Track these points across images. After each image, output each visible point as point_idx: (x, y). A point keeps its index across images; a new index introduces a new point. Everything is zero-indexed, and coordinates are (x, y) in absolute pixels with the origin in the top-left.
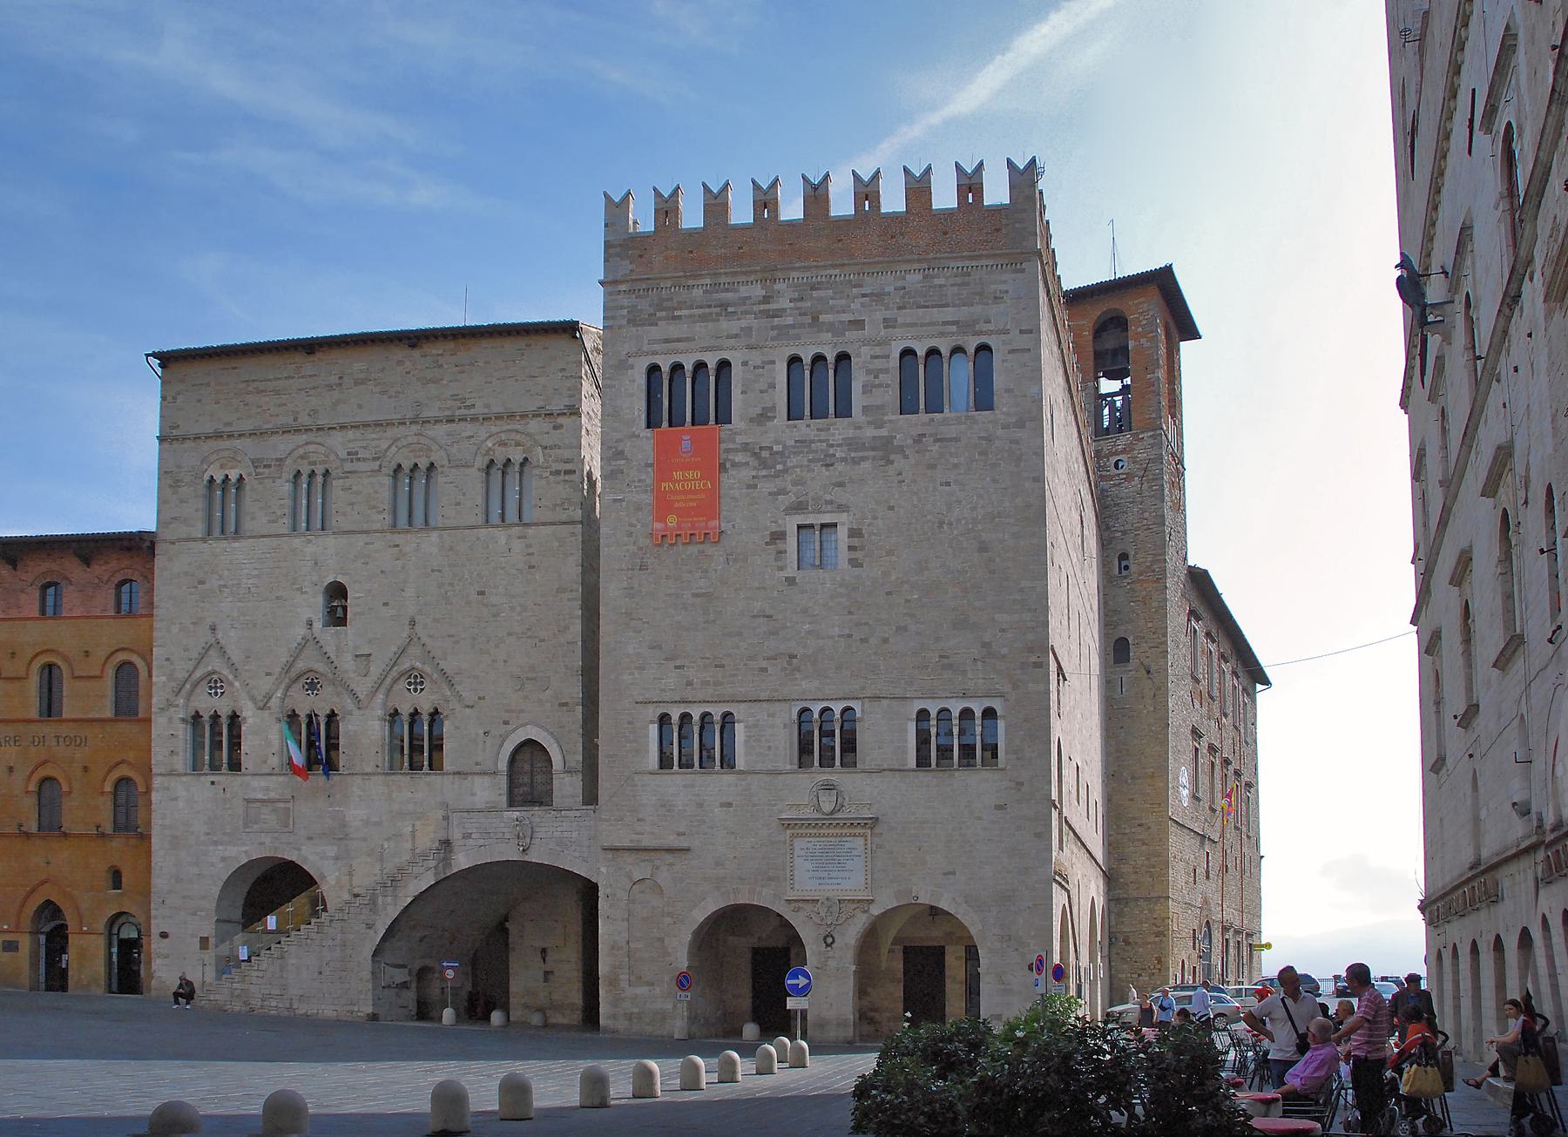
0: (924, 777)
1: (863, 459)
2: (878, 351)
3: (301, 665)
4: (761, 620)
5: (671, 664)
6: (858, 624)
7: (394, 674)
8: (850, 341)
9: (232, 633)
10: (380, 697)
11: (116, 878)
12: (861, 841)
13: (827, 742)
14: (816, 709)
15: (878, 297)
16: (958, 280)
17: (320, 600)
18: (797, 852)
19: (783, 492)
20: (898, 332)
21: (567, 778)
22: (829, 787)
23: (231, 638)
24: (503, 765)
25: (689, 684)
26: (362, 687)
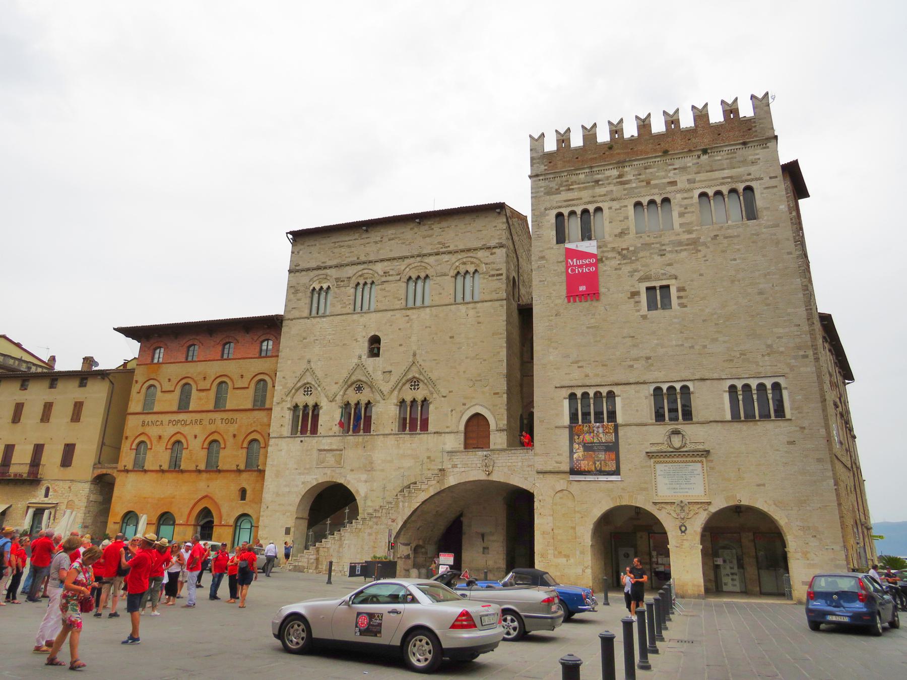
0: (736, 425)
1: (681, 250)
2: (685, 195)
3: (354, 378)
4: (627, 339)
5: (576, 365)
6: (686, 339)
7: (404, 381)
8: (669, 192)
9: (319, 363)
11: (243, 493)
12: (699, 465)
13: (673, 405)
14: (665, 387)
15: (684, 169)
16: (730, 156)
17: (366, 344)
18: (658, 472)
19: (636, 271)
20: (697, 185)
21: (498, 434)
22: (676, 432)
23: (319, 367)
24: (462, 427)
25: (587, 376)
26: (386, 388)
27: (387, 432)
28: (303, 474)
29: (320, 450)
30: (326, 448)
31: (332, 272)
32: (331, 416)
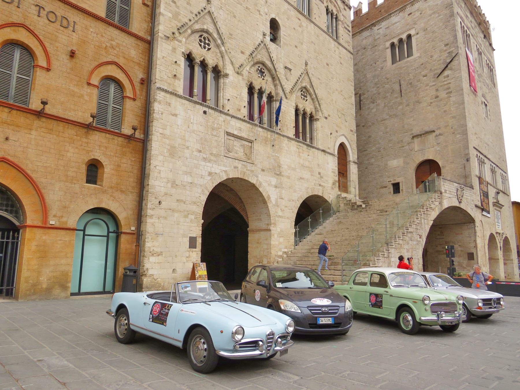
24: (336, 153)
28: (210, 161)
29: (228, 134)
30: (236, 133)
32: (234, 92)
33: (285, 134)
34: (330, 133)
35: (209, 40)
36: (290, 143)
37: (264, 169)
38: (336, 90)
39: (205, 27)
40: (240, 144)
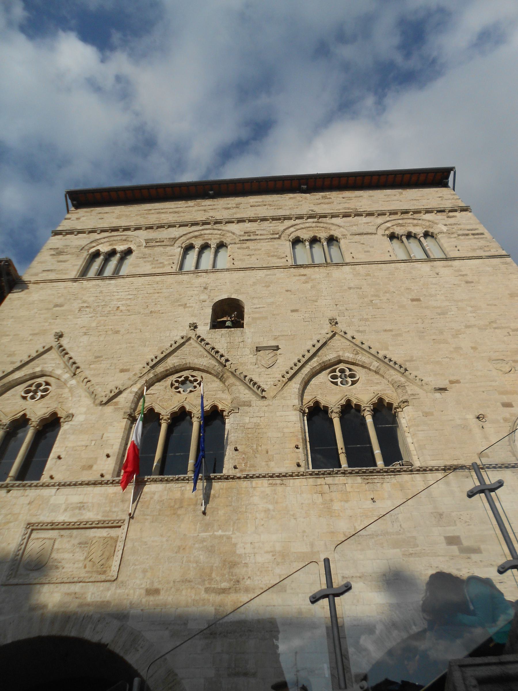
7: (314, 363)
9: (85, 339)
10: (295, 385)
27: (283, 470)
30: (62, 518)
31: (143, 234)
33: (257, 473)
34: (471, 417)
35: (47, 384)
36: (280, 489)
37: (156, 585)
38: (468, 327)
39: (38, 369)
40: (76, 542)
